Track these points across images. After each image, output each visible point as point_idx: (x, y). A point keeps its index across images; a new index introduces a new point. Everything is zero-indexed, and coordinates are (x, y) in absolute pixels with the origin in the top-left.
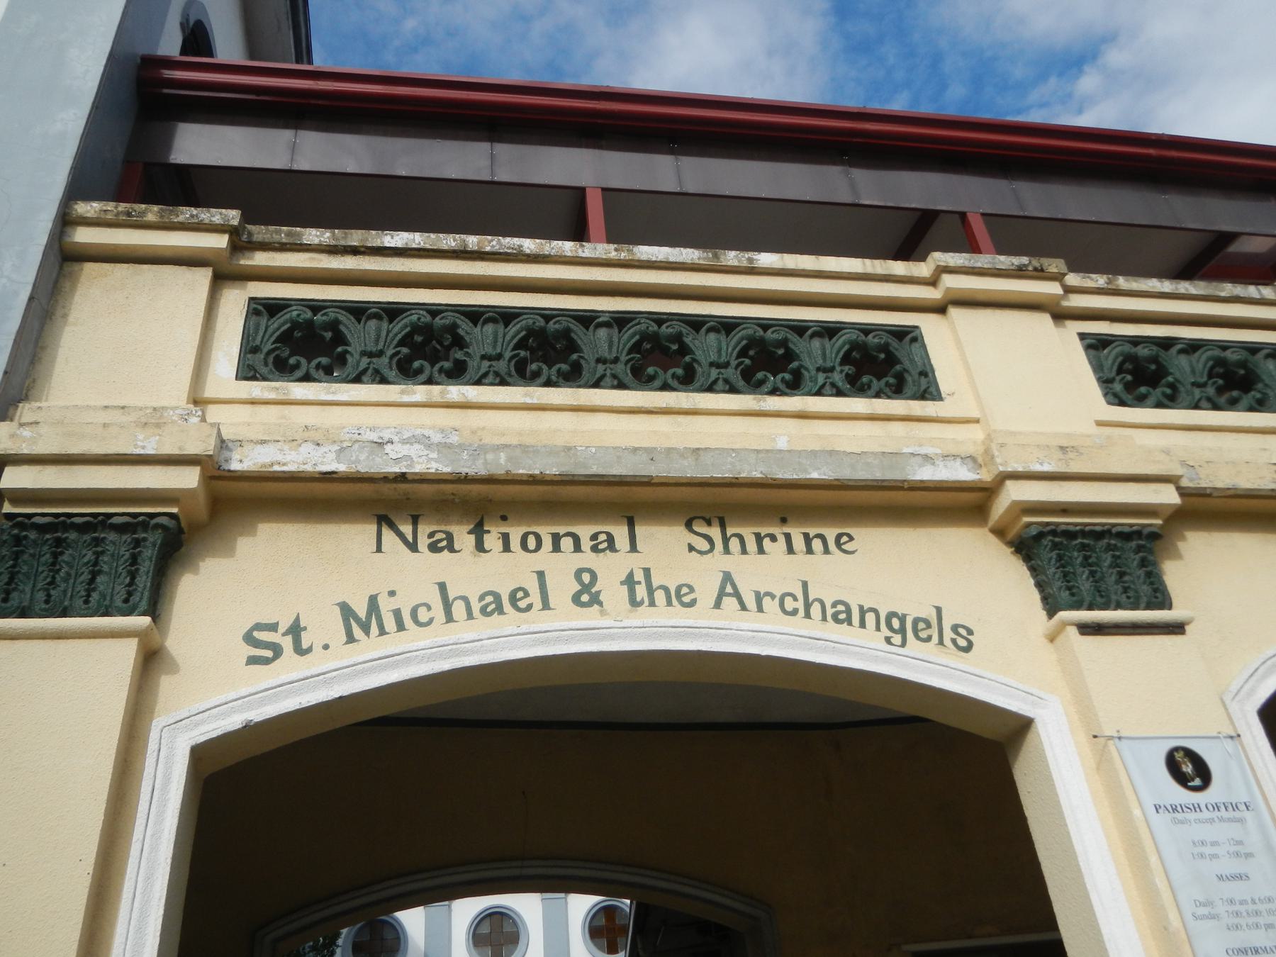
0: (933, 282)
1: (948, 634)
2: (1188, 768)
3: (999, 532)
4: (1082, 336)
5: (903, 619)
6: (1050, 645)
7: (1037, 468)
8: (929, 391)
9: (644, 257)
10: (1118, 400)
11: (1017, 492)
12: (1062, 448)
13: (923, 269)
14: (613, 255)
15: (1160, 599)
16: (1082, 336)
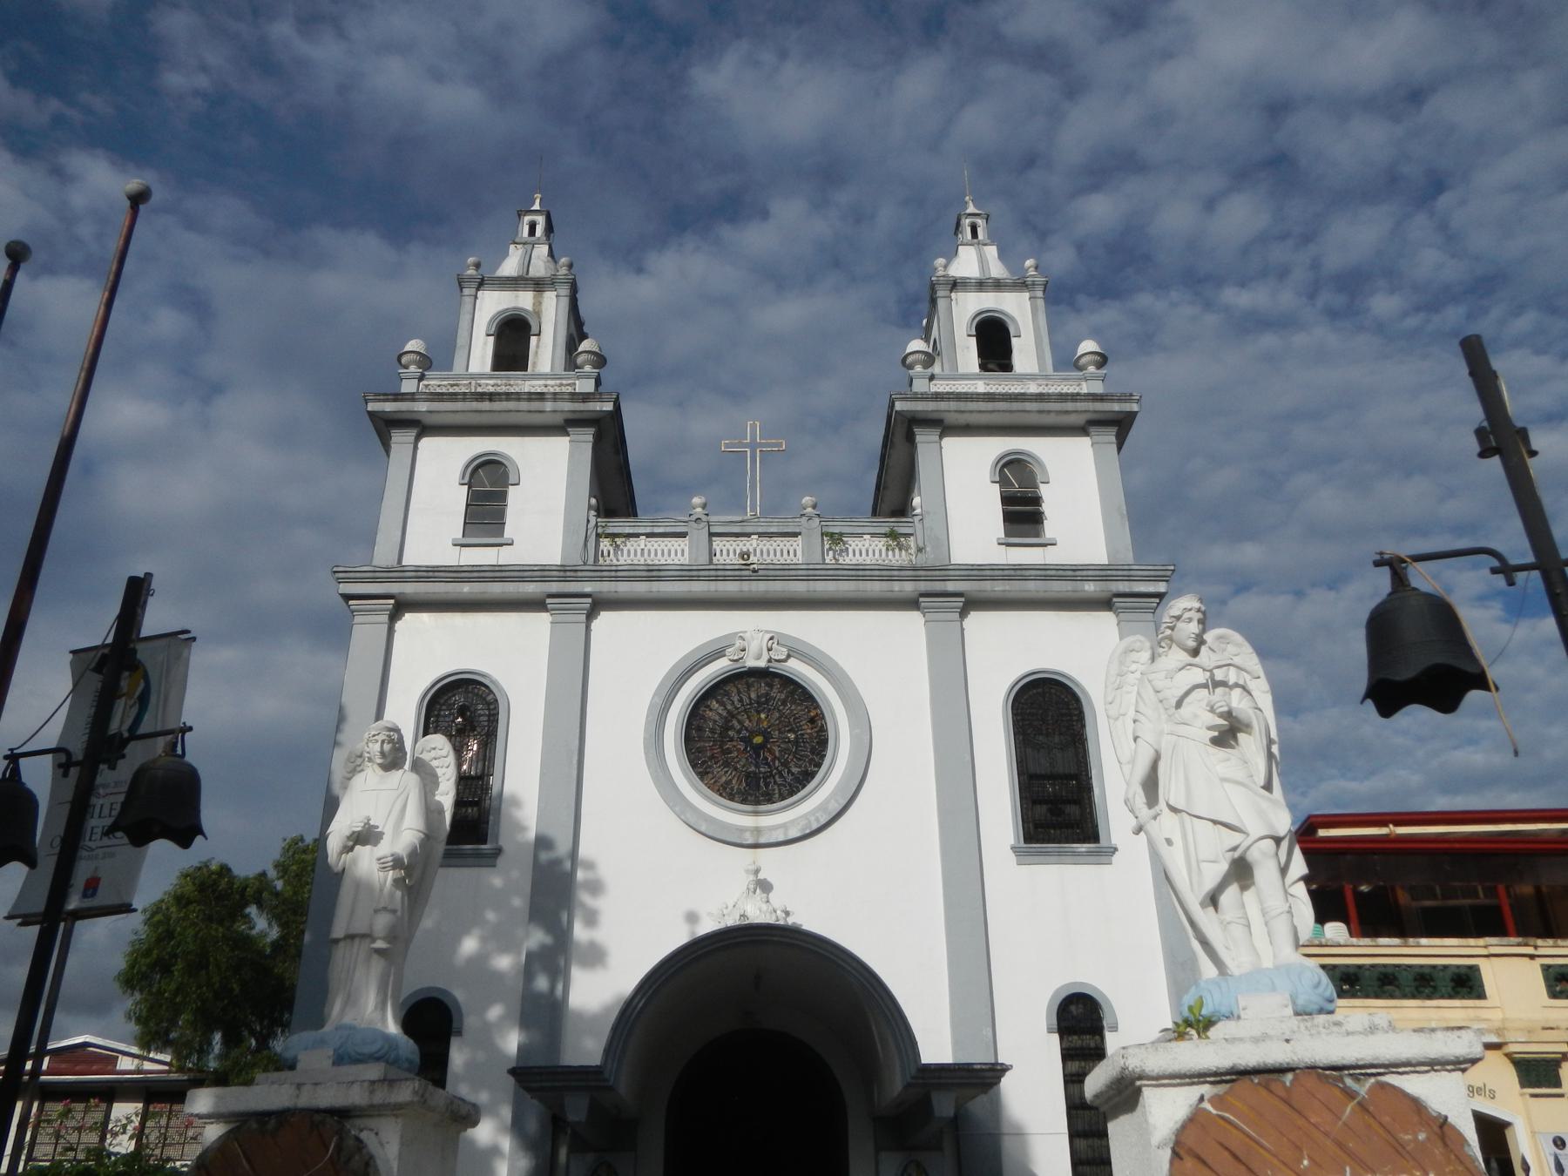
0: (1486, 947)
1: (1487, 1092)
2: (1559, 1143)
3: (1508, 1055)
4: (1542, 965)
5: (1473, 1087)
6: (1520, 1098)
7: (1520, 1040)
8: (1481, 995)
9: (1381, 944)
10: (1554, 995)
11: (1512, 1048)
12: (1529, 1032)
13: (1481, 942)
14: (1371, 944)
15: (1558, 1084)
16: (1542, 965)
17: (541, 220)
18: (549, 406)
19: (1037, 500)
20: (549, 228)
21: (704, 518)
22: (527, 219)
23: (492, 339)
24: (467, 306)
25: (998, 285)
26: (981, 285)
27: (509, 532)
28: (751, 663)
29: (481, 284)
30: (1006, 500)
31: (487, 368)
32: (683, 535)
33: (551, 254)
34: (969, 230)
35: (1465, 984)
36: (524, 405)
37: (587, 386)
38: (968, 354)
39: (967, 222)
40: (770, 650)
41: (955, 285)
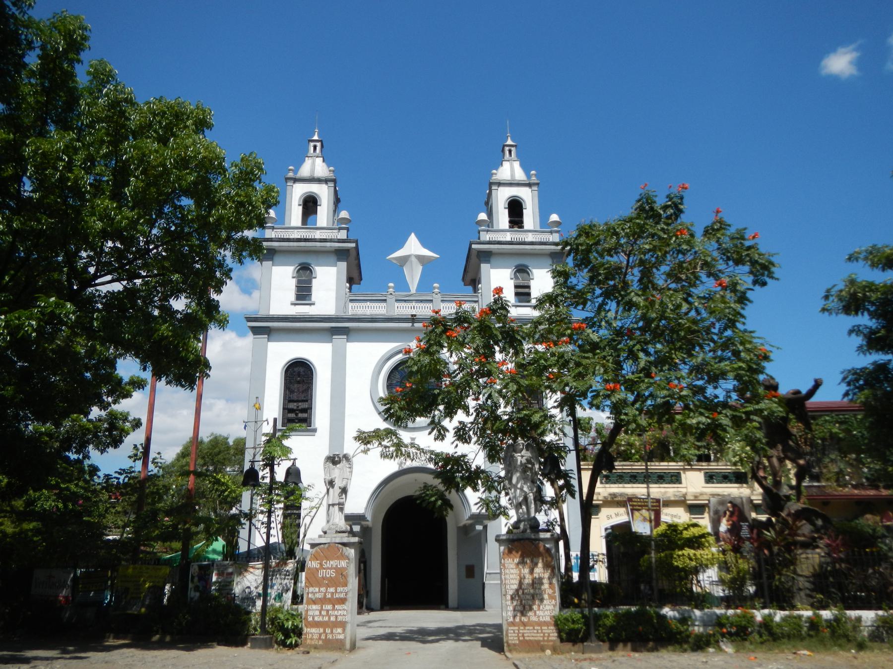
8: (680, 483)
11: (689, 502)
17: (319, 144)
18: (328, 244)
19: (529, 287)
20: (322, 146)
22: (312, 144)
23: (301, 208)
24: (288, 192)
25: (519, 184)
26: (510, 184)
27: (314, 297)
29: (296, 180)
30: (516, 287)
31: (299, 224)
32: (385, 301)
33: (324, 161)
34: (507, 153)
35: (675, 478)
36: (318, 244)
37: (343, 235)
38: (503, 218)
39: (507, 149)
41: (500, 184)
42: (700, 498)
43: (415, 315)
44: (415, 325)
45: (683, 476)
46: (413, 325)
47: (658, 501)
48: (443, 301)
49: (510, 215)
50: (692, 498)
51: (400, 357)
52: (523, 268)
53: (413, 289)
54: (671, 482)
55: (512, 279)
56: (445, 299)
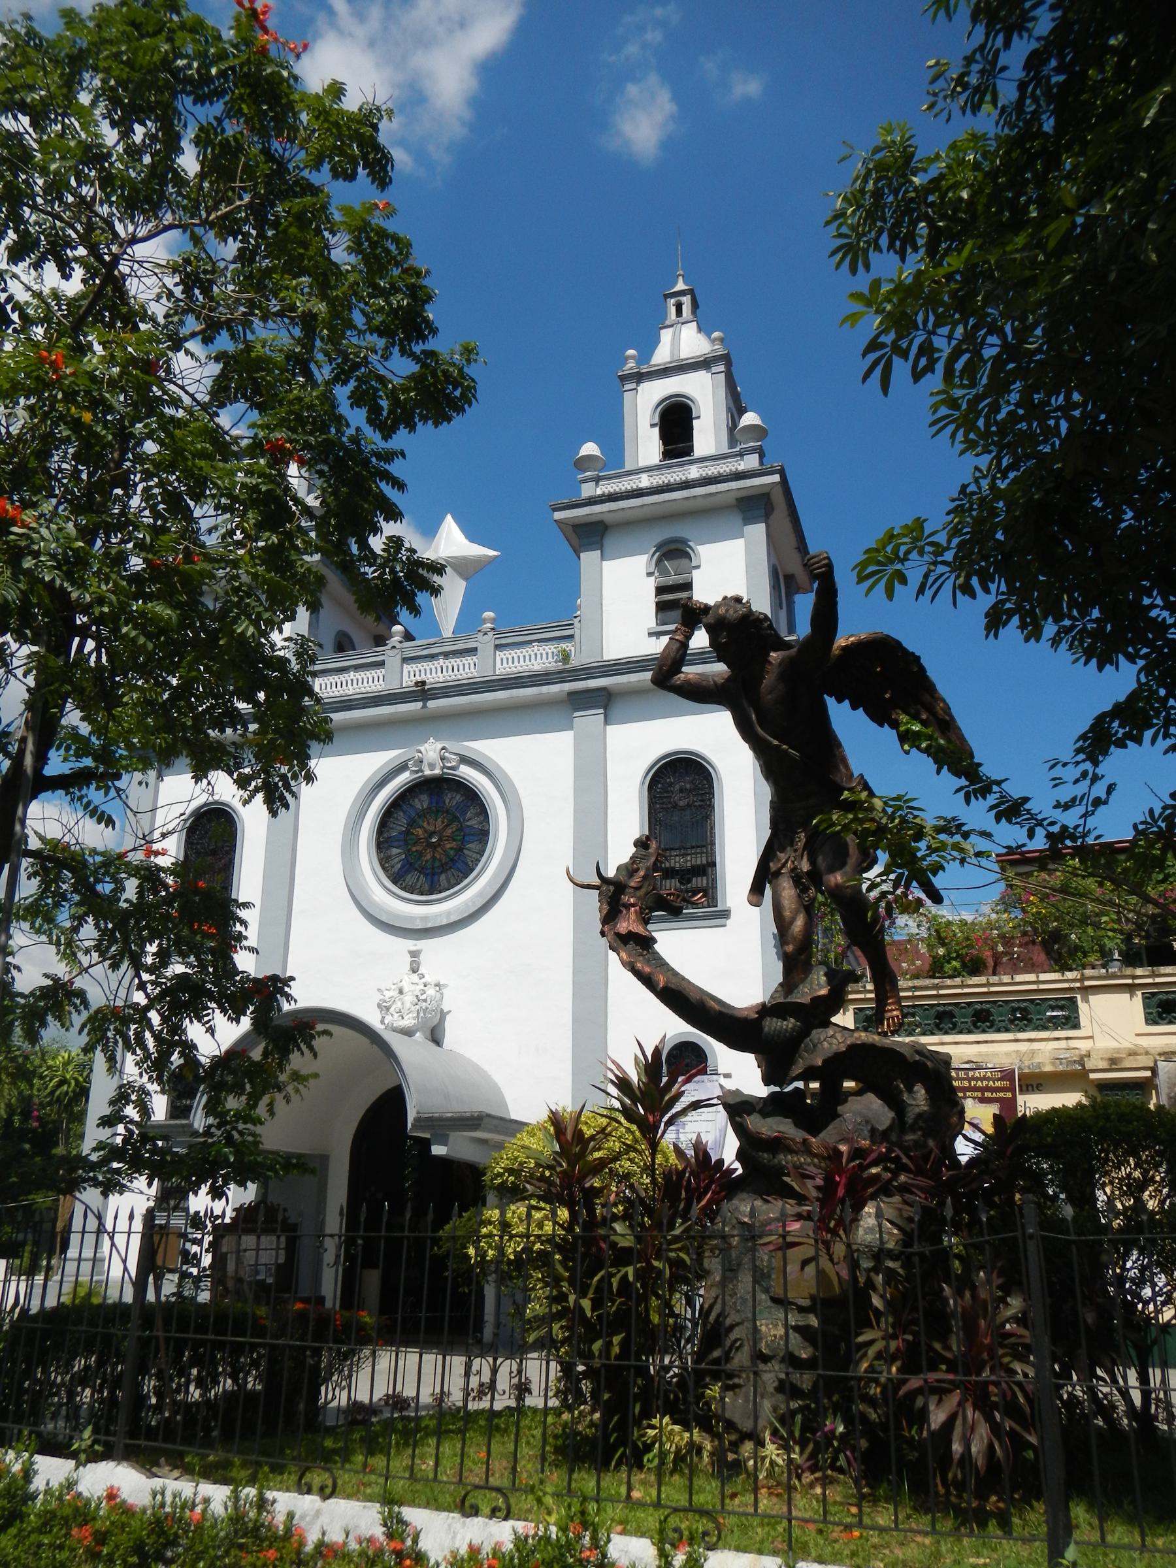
8: (1076, 1026)
11: (1092, 1076)
21: (398, 645)
28: (428, 772)
30: (660, 590)
40: (443, 759)
42: (1127, 1064)
43: (423, 683)
44: (431, 704)
45: (1081, 1005)
46: (424, 706)
47: (1008, 1075)
48: (498, 647)
49: (665, 437)
50: (1103, 1065)
51: (404, 777)
52: (679, 546)
53: (447, 632)
54: (1056, 1024)
55: (650, 574)
56: (503, 641)
